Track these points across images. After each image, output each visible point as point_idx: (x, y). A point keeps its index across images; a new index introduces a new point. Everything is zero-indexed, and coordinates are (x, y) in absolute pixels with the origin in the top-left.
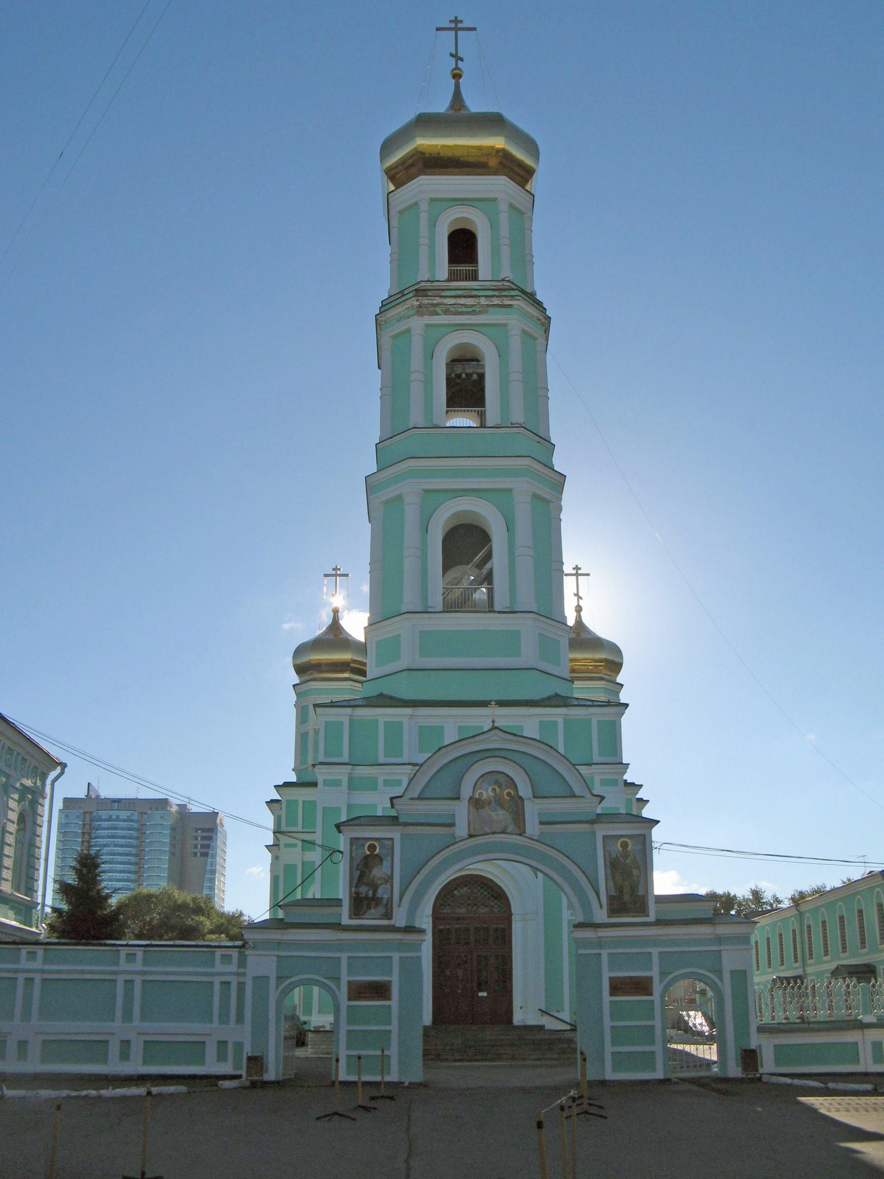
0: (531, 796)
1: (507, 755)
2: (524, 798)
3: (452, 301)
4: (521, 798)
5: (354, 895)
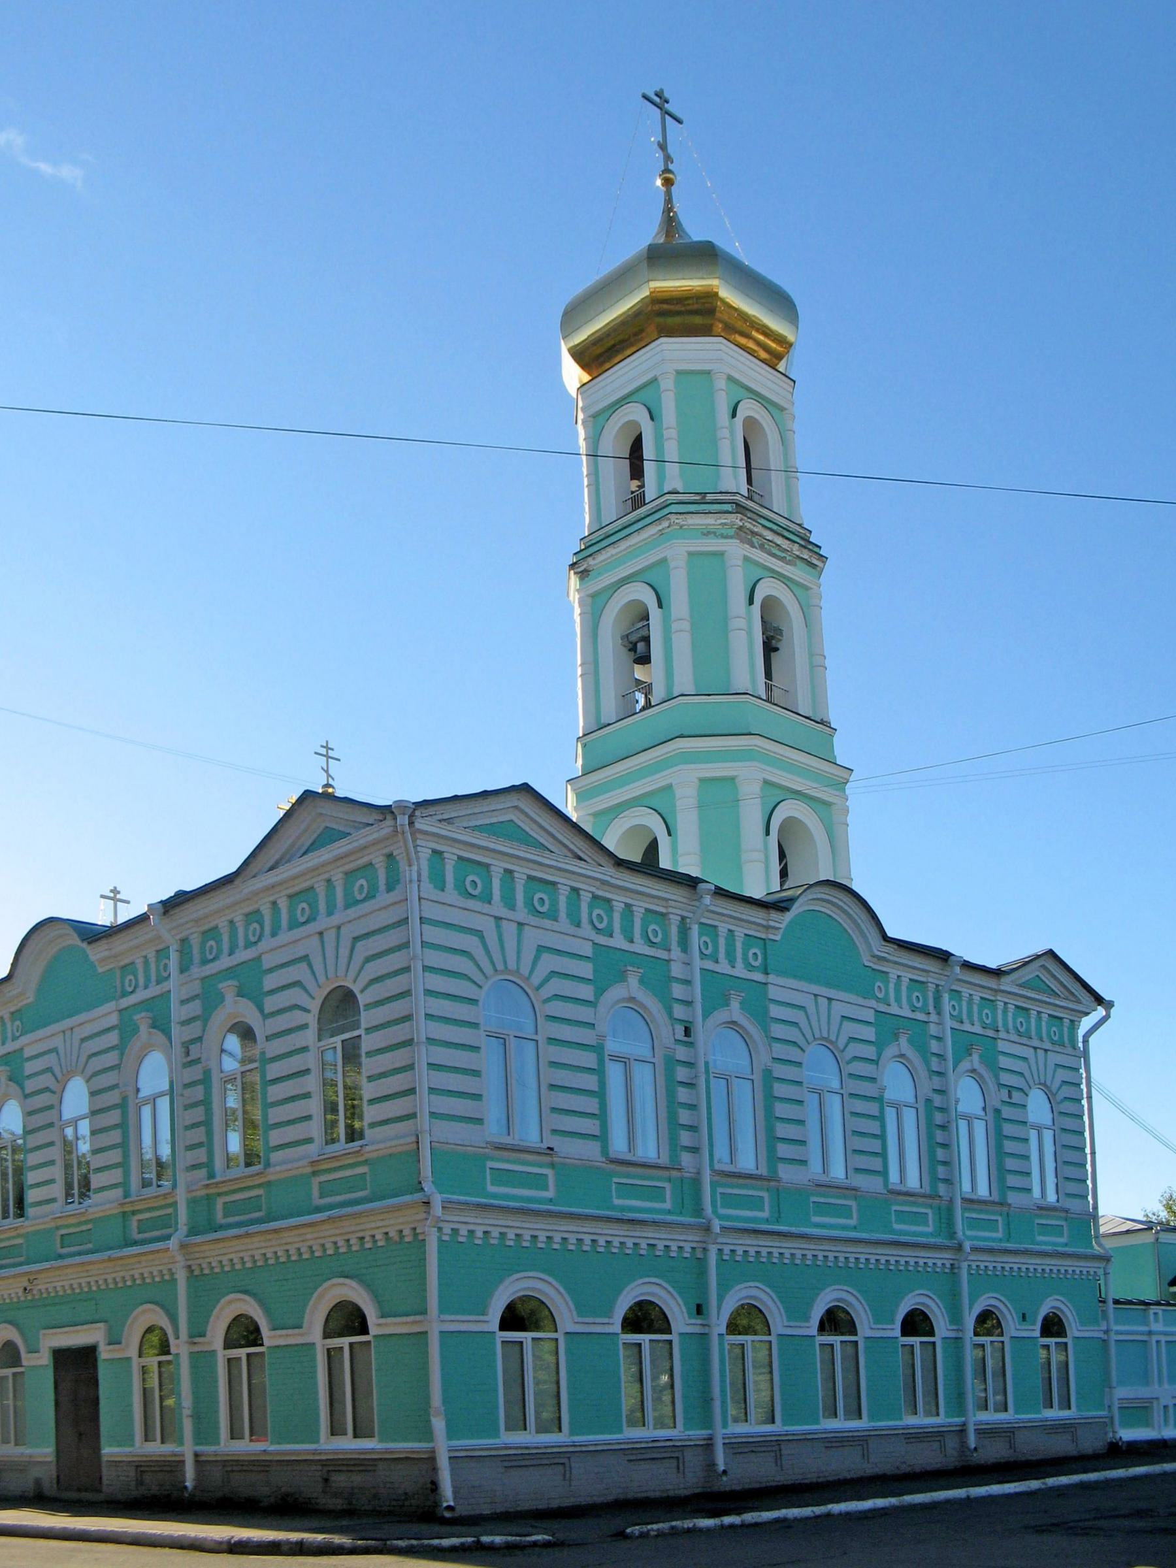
3: (769, 535)
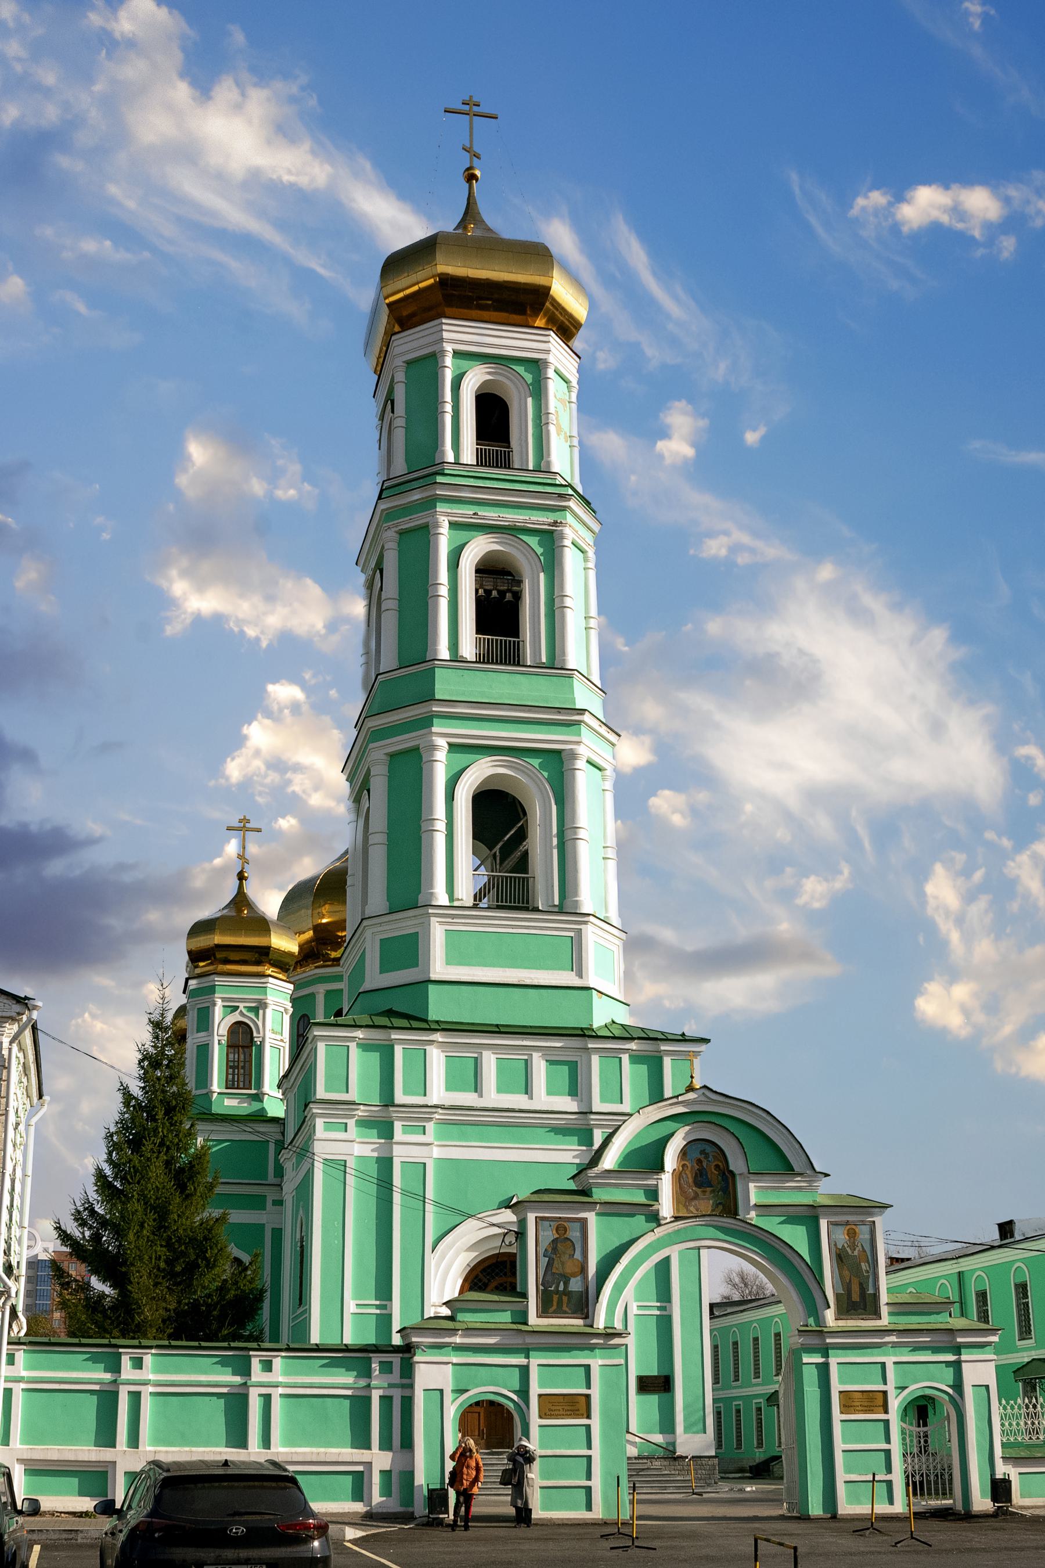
0: (744, 1170)
1: (713, 1119)
2: (736, 1172)
4: (732, 1173)
5: (541, 1288)
